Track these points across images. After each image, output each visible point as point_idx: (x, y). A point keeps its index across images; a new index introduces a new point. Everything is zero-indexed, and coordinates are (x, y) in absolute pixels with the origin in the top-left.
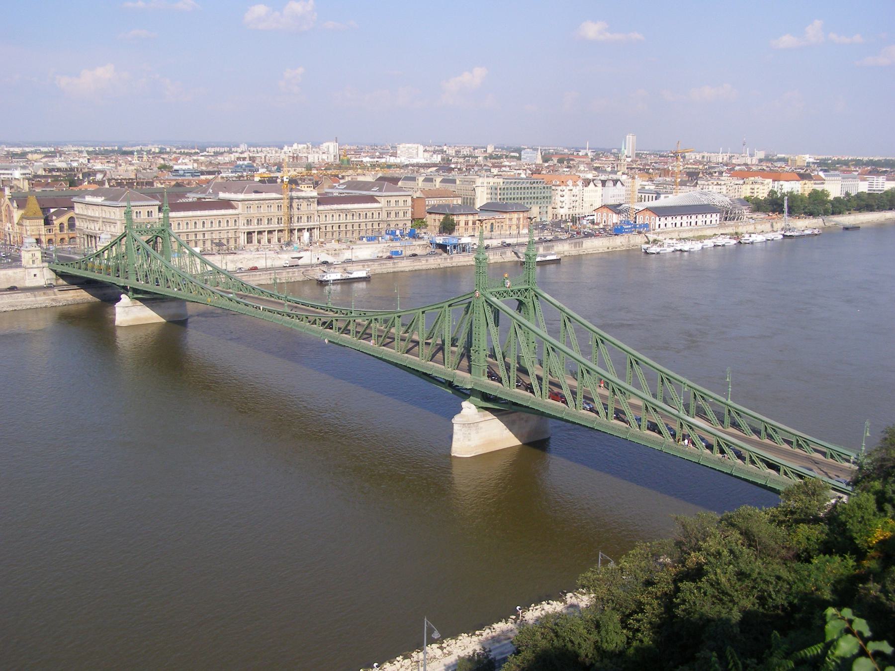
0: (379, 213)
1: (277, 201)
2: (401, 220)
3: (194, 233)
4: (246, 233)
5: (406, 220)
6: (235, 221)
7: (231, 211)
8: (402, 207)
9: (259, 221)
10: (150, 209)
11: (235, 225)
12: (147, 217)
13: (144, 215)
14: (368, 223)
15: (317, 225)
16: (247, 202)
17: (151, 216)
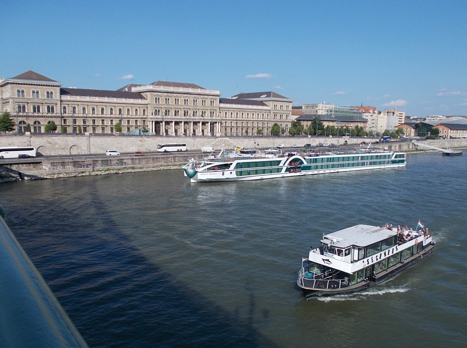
0: (268, 115)
1: (184, 95)
2: (284, 122)
3: (101, 119)
4: (154, 123)
5: (287, 122)
6: (144, 110)
7: (140, 101)
8: (285, 111)
9: (167, 112)
10: (50, 89)
11: (144, 114)
12: (46, 97)
13: (43, 95)
14: (260, 122)
15: (219, 120)
16: (155, 94)
17: (52, 97)
